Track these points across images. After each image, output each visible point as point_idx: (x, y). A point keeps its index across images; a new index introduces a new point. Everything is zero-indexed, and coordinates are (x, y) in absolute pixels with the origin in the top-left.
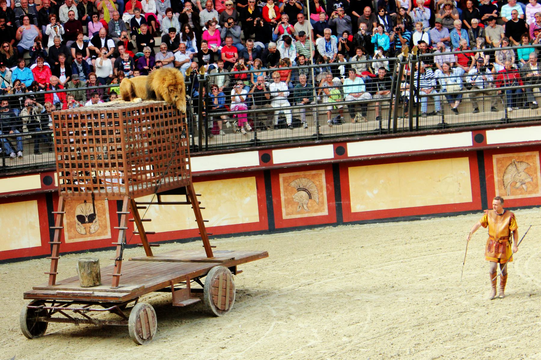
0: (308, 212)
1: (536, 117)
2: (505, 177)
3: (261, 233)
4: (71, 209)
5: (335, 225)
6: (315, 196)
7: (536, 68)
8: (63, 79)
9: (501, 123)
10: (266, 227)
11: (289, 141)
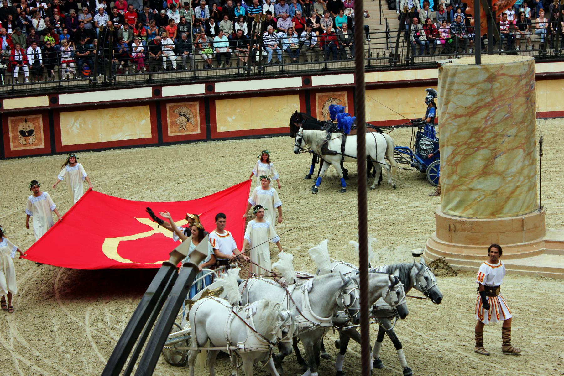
0: (186, 131)
1: (346, 68)
2: (324, 109)
3: (153, 145)
4: (15, 126)
5: (205, 141)
6: (192, 120)
7: (346, 33)
8: (10, 31)
9: (322, 71)
10: (156, 141)
11: (174, 81)
